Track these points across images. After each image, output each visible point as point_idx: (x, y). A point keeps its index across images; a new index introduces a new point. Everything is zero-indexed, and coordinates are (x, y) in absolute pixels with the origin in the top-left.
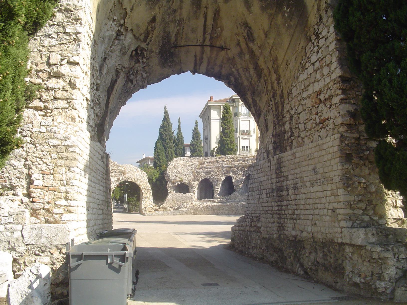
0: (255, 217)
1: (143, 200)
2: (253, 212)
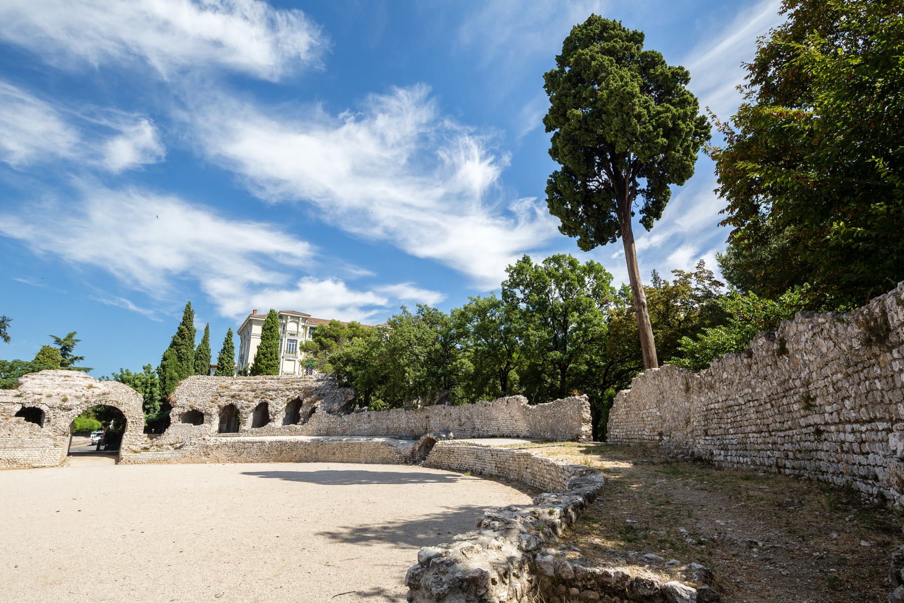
1: (126, 433)
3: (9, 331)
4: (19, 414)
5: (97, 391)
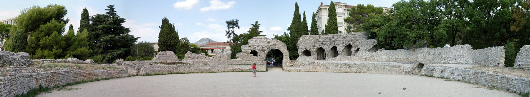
3: (239, 25)
4: (251, 53)
5: (272, 44)
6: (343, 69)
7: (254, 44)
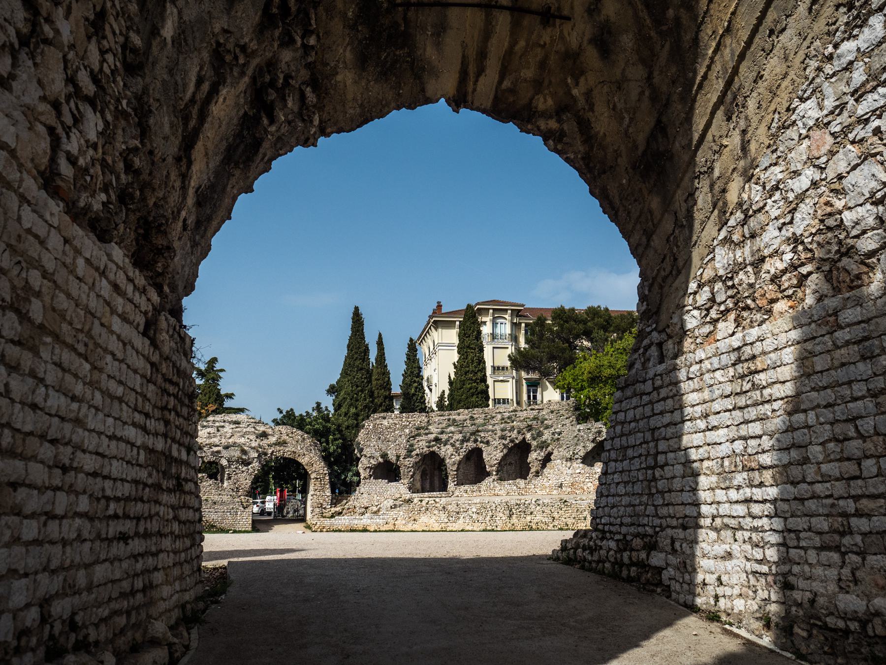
0: (637, 535)
2: (627, 520)
5: (273, 439)
6: (501, 519)
7: (216, 440)
